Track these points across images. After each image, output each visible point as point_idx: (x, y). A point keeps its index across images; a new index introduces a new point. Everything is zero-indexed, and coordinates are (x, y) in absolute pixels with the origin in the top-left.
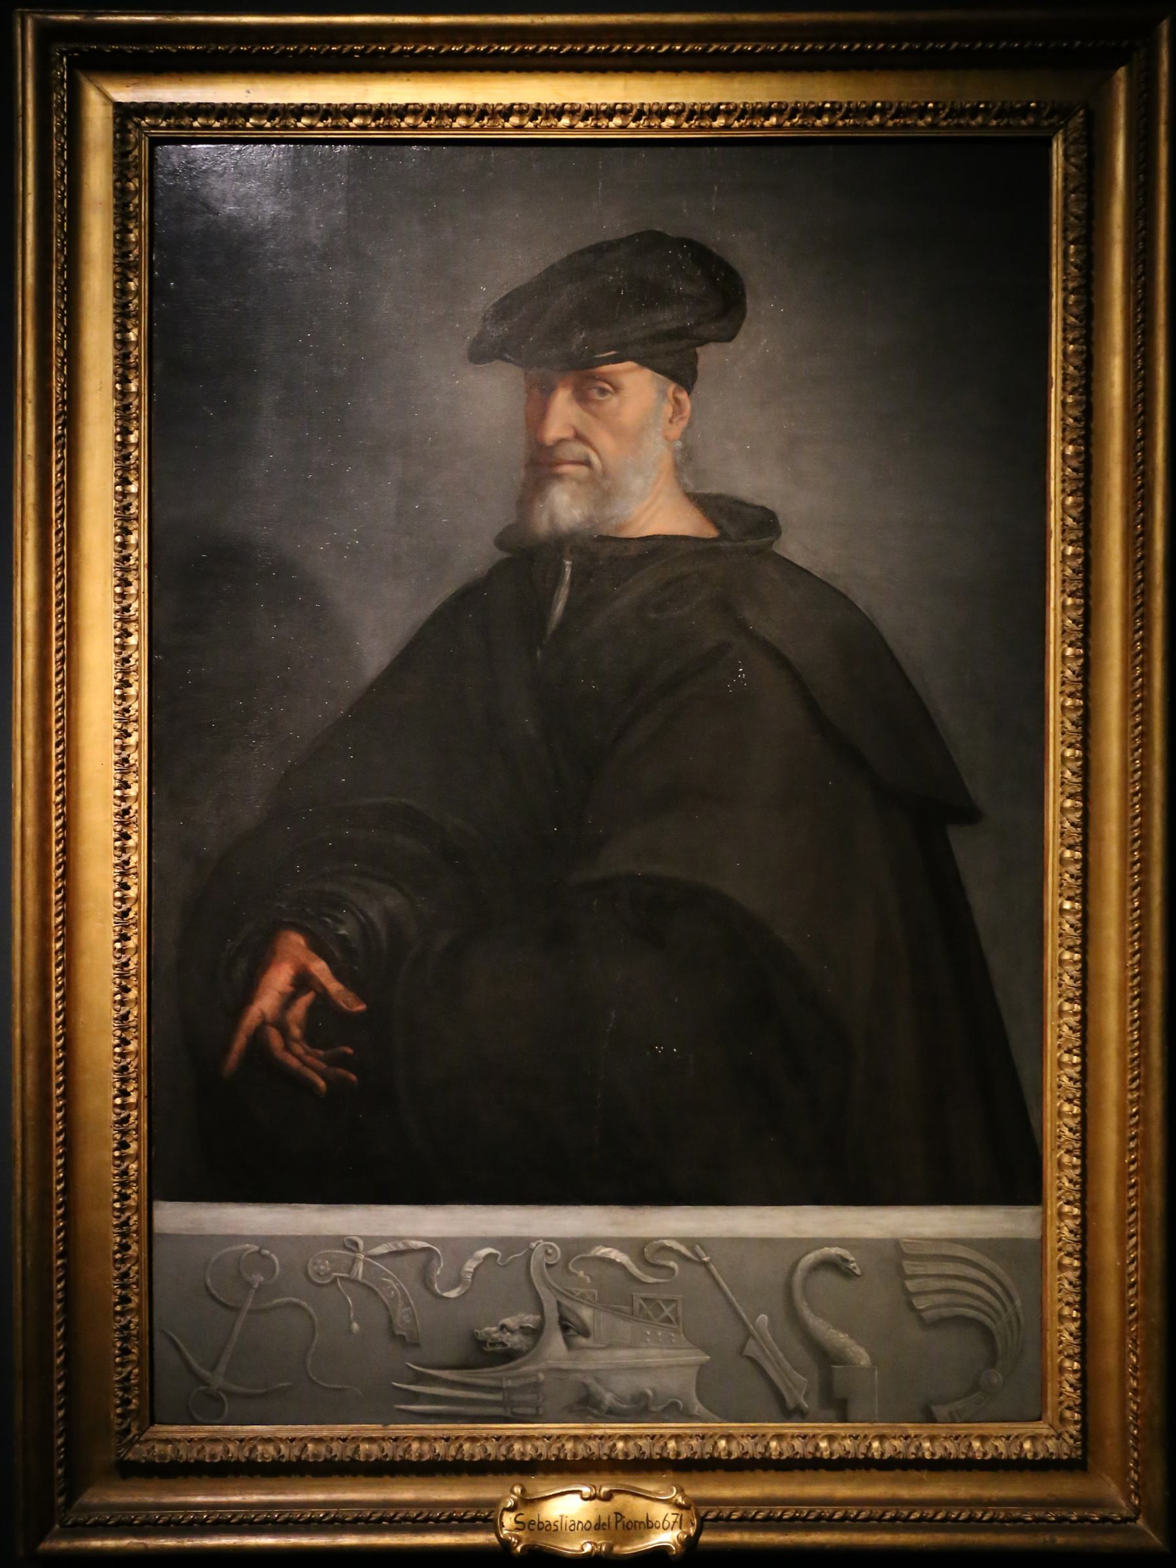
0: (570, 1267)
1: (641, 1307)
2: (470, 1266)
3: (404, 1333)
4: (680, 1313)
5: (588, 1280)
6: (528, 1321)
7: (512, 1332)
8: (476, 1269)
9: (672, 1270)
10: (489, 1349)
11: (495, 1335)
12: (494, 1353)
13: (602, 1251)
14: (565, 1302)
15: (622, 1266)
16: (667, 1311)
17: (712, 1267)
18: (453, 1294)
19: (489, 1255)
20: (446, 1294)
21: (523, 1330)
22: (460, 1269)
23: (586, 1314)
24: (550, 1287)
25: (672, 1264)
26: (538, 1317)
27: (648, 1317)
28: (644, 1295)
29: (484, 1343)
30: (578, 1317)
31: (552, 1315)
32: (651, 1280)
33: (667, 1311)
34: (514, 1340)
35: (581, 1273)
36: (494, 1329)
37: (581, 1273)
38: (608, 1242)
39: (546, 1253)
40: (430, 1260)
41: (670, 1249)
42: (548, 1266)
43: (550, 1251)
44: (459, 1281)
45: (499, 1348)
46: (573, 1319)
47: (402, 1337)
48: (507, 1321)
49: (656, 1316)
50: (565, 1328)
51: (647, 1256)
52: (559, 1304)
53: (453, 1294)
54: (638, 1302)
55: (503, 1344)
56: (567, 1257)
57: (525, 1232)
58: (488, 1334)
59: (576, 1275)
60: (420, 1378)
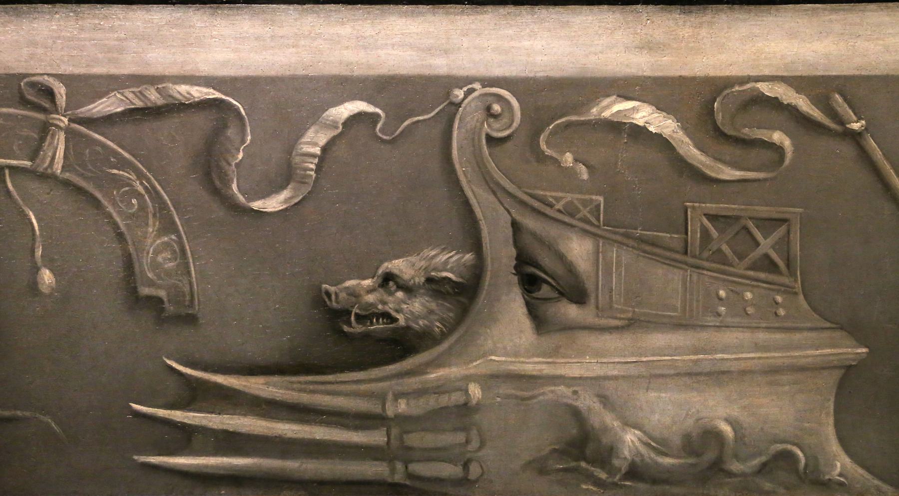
0: (543, 146)
1: (705, 233)
2: (313, 141)
3: (162, 293)
4: (796, 248)
5: (584, 173)
6: (444, 266)
7: (409, 290)
8: (324, 149)
9: (779, 149)
10: (358, 329)
11: (370, 298)
12: (366, 336)
13: (615, 108)
14: (530, 222)
15: (661, 142)
16: (766, 244)
17: (871, 144)
18: (273, 204)
19: (357, 118)
20: (257, 205)
21: (435, 286)
22: (290, 148)
23: (578, 249)
24: (495, 188)
25: (777, 137)
26: (469, 257)
27: (720, 257)
28: (711, 207)
29: (343, 314)
30: (561, 257)
31: (500, 254)
32: (729, 173)
33: (766, 244)
34: (413, 310)
35: (568, 159)
36: (368, 282)
37: (568, 159)
38: (625, 87)
39: (489, 113)
40: (219, 130)
41: (775, 104)
42: (490, 139)
43: (497, 108)
44: (286, 175)
45: (378, 326)
46: (546, 260)
47: (155, 303)
48: (399, 266)
49: (741, 257)
50: (530, 282)
51: (719, 117)
52: (516, 226)
53: (273, 204)
54: (697, 223)
55: (387, 316)
56: (536, 122)
57: (440, 65)
58: (354, 294)
59: (556, 162)
60: (195, 395)
